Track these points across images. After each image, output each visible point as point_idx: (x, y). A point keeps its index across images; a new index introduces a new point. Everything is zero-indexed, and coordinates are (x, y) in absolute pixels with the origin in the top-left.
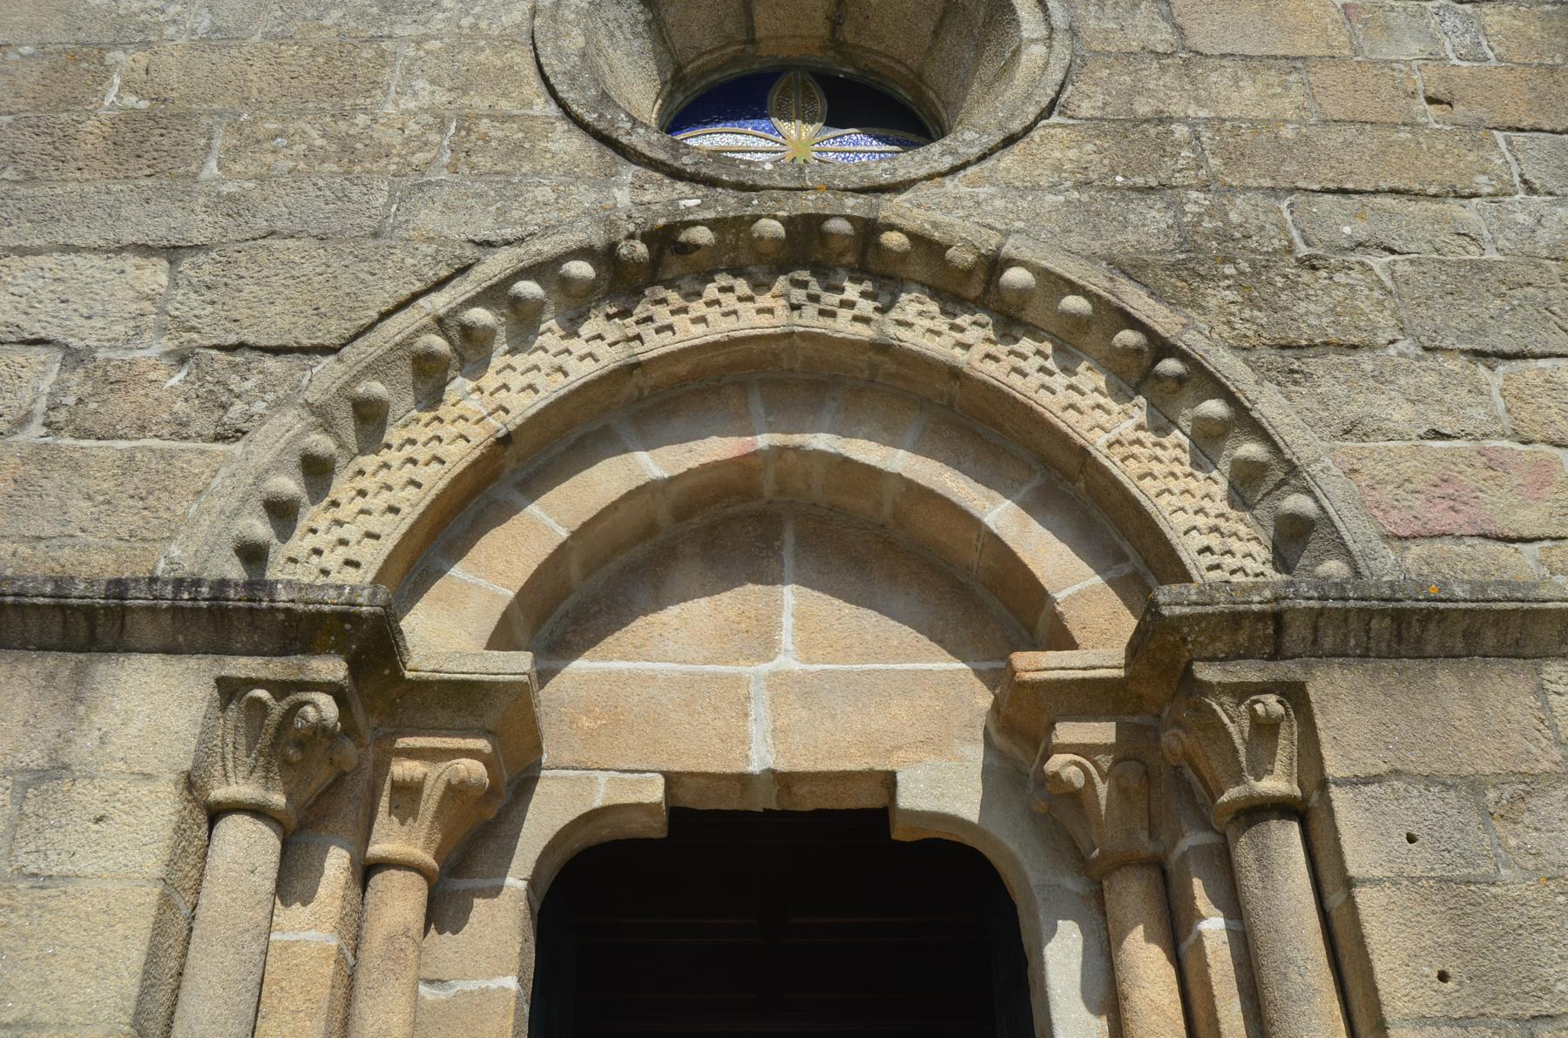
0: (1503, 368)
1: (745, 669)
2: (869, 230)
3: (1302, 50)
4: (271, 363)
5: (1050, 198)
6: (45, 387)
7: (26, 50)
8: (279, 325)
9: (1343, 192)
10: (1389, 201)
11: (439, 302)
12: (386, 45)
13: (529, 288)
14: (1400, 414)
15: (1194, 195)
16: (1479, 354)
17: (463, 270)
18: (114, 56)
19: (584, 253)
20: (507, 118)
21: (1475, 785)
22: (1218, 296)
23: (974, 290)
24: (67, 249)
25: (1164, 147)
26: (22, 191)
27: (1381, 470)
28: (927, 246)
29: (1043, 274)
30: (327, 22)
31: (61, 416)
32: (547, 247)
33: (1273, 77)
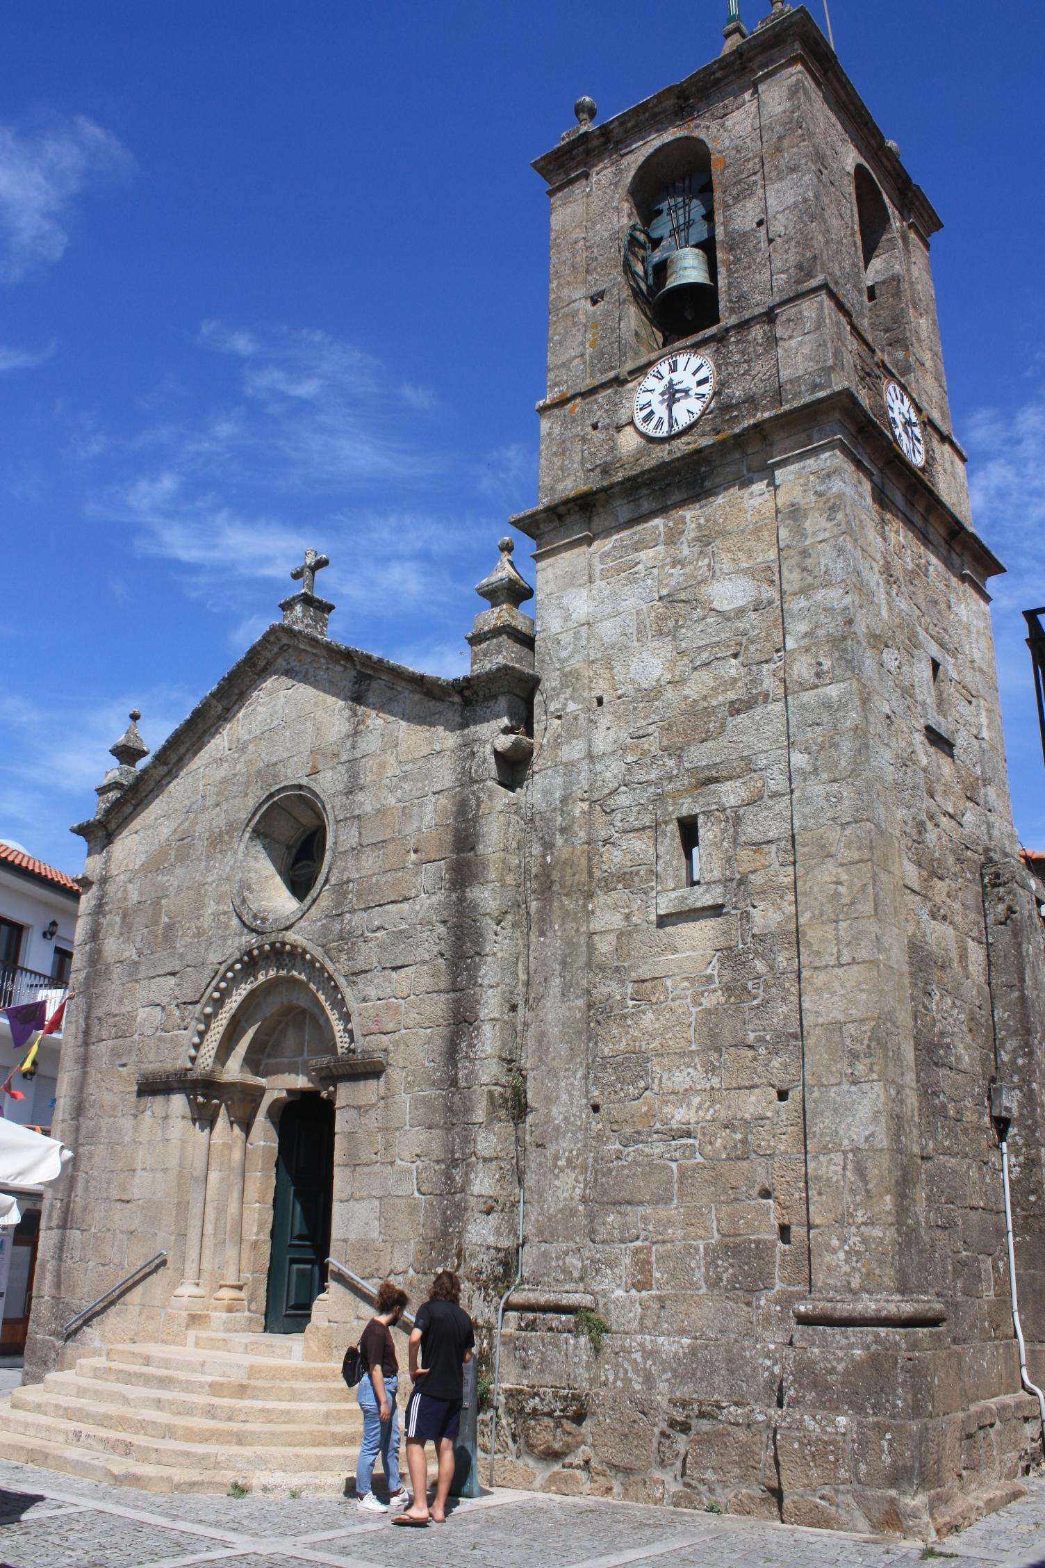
1: (299, 1059)
2: (284, 944)
9: (380, 905)
10: (390, 906)
11: (214, 983)
13: (230, 975)
14: (373, 993)
16: (394, 969)
17: (217, 973)
19: (237, 961)
21: (359, 1108)
32: (230, 962)
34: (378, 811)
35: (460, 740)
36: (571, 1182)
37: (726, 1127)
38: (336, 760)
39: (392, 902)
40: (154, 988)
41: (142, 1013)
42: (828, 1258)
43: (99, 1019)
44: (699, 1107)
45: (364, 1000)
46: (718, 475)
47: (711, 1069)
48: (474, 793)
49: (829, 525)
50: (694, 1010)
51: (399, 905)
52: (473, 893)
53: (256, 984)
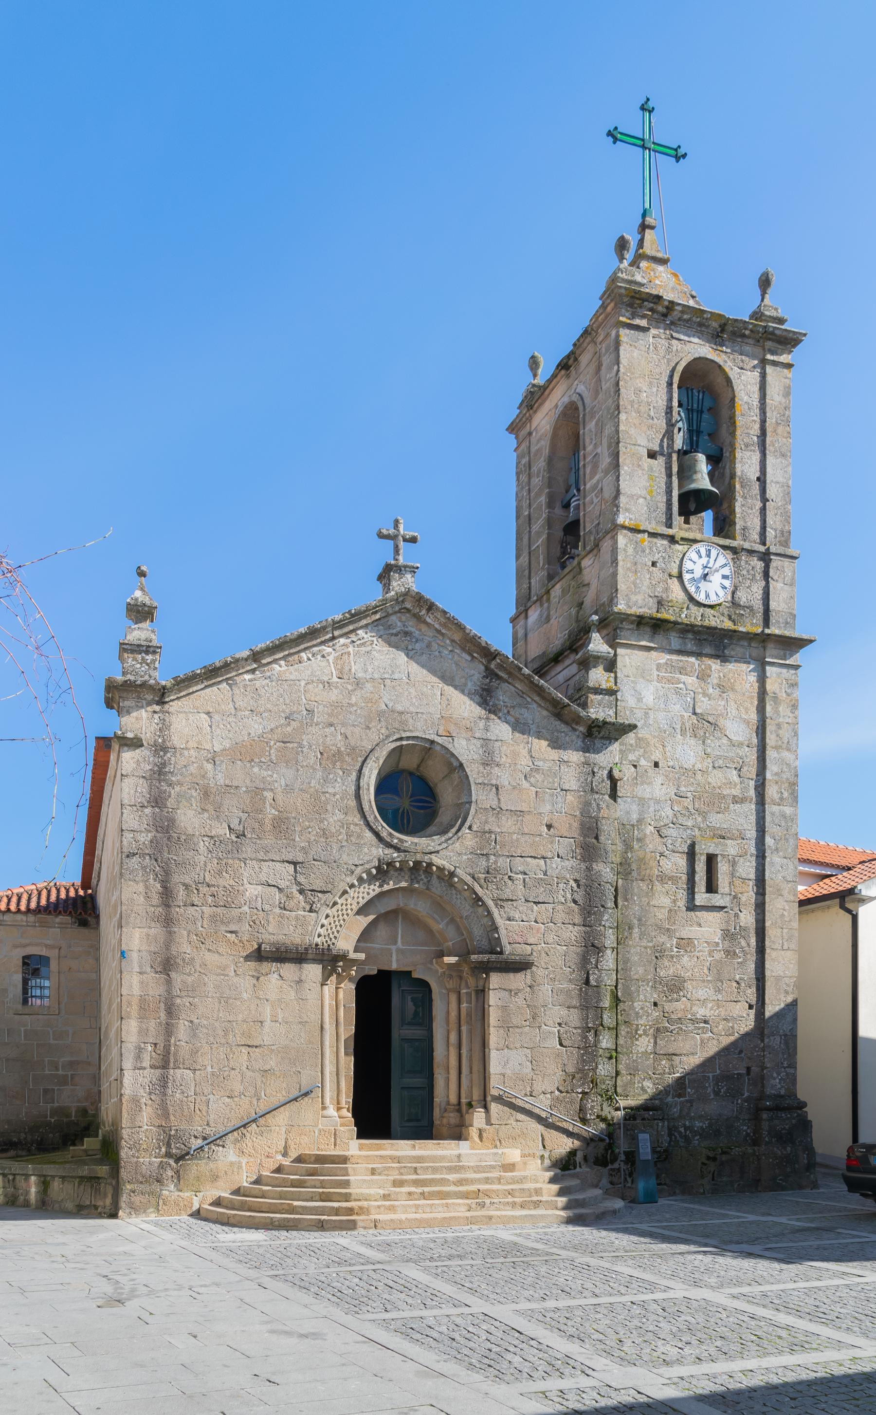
0: (539, 905)
2: (430, 864)
3: (524, 809)
4: (319, 895)
5: (465, 857)
6: (277, 898)
7: (244, 789)
8: (318, 884)
9: (521, 857)
12: (327, 795)
15: (492, 857)
18: (265, 793)
19: (375, 867)
20: (356, 825)
22: (492, 887)
23: (446, 878)
24: (273, 861)
25: (488, 841)
26: (258, 842)
27: (511, 929)
28: (441, 869)
29: (461, 880)
30: (312, 785)
31: (282, 905)
32: (367, 866)
33: (515, 818)
34: (514, 788)
35: (583, 759)
36: (646, 1042)
37: (724, 1020)
38: (470, 733)
39: (531, 857)
40: (265, 869)
41: (252, 891)
42: (772, 1082)
43: (187, 886)
44: (711, 1009)
45: (509, 919)
46: (733, 649)
47: (718, 991)
48: (595, 800)
49: (791, 715)
50: (709, 959)
51: (537, 860)
52: (598, 867)
53: (386, 888)
